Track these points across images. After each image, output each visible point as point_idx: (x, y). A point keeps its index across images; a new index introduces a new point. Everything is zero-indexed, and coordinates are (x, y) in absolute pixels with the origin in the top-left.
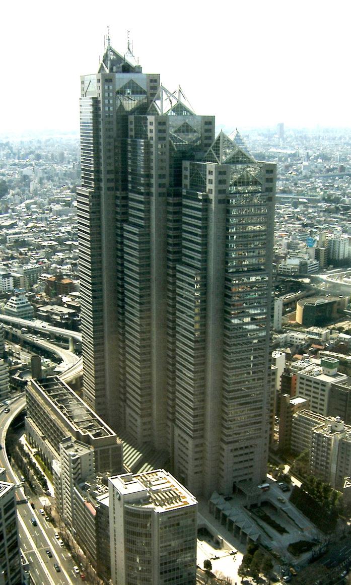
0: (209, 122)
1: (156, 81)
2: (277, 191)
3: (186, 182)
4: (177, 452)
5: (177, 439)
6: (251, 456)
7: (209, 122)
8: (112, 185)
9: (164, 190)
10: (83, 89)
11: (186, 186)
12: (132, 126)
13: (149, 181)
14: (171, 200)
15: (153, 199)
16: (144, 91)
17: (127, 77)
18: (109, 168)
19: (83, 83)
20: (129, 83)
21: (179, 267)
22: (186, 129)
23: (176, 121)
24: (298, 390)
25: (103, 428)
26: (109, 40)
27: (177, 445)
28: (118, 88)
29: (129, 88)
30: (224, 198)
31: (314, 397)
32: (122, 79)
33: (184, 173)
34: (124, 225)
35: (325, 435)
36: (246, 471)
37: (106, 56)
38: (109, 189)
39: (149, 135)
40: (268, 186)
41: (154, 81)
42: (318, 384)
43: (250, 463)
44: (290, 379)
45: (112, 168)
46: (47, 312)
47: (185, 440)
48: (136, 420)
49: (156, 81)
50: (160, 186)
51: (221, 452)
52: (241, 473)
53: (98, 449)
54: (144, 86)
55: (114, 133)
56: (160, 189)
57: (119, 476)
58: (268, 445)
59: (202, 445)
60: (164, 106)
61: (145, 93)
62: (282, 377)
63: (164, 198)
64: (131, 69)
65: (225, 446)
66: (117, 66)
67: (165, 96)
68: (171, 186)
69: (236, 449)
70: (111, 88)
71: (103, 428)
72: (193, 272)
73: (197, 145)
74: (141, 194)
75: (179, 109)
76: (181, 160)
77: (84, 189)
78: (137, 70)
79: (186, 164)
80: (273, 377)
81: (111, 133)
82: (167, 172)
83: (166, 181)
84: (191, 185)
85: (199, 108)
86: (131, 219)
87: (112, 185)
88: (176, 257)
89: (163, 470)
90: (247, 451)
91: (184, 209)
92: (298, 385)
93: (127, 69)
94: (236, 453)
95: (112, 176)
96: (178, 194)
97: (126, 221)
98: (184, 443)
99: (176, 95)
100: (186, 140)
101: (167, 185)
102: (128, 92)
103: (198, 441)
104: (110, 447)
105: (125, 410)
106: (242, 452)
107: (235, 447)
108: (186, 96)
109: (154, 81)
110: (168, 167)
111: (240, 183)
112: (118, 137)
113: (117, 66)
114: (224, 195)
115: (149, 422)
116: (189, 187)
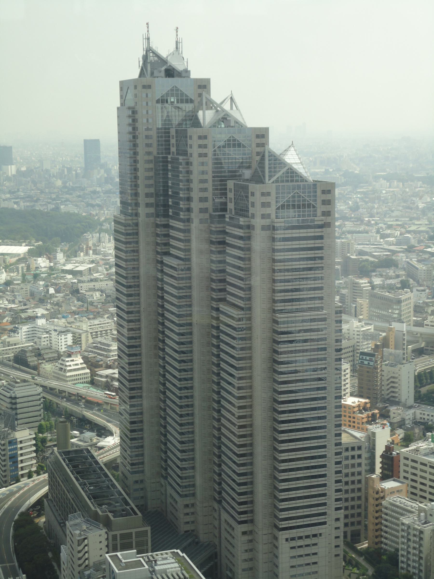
0: (262, 135)
2: (337, 216)
5: (224, 526)
6: (313, 550)
7: (262, 135)
10: (121, 97)
11: (231, 210)
12: (173, 141)
13: (189, 204)
16: (191, 99)
17: (171, 82)
18: (148, 190)
19: (121, 89)
20: (172, 90)
21: (223, 307)
22: (233, 143)
23: (221, 135)
25: (128, 507)
26: (148, 39)
27: (224, 534)
28: (158, 97)
29: (172, 95)
30: (268, 224)
31: (412, 480)
32: (163, 85)
34: (164, 258)
35: (416, 526)
37: (145, 58)
40: (325, 210)
41: (204, 85)
42: (426, 465)
43: (313, 559)
44: (392, 459)
45: (152, 190)
46: (107, 376)
47: (231, 526)
48: (176, 502)
51: (275, 541)
53: (118, 533)
54: (190, 92)
55: (154, 150)
56: (202, 214)
57: (119, 554)
59: (251, 532)
60: (206, 116)
61: (192, 101)
62: (382, 456)
63: (206, 225)
65: (276, 531)
66: (158, 69)
69: (293, 539)
70: (149, 96)
71: (128, 507)
72: (235, 312)
73: (248, 161)
76: (226, 181)
78: (184, 75)
79: (230, 184)
81: (151, 149)
83: (209, 205)
84: (235, 209)
85: (251, 119)
87: (152, 210)
88: (221, 295)
89: (179, 551)
90: (308, 541)
92: (402, 468)
93: (170, 73)
94: (293, 544)
95: (152, 200)
97: (167, 254)
100: (236, 155)
101: (211, 210)
102: (172, 100)
104: (133, 531)
105: (220, 515)
106: (300, 543)
107: (292, 536)
109: (204, 85)
111: (288, 206)
112: (158, 153)
113: (158, 69)
114: (268, 220)
115: (193, 505)
116: (233, 213)
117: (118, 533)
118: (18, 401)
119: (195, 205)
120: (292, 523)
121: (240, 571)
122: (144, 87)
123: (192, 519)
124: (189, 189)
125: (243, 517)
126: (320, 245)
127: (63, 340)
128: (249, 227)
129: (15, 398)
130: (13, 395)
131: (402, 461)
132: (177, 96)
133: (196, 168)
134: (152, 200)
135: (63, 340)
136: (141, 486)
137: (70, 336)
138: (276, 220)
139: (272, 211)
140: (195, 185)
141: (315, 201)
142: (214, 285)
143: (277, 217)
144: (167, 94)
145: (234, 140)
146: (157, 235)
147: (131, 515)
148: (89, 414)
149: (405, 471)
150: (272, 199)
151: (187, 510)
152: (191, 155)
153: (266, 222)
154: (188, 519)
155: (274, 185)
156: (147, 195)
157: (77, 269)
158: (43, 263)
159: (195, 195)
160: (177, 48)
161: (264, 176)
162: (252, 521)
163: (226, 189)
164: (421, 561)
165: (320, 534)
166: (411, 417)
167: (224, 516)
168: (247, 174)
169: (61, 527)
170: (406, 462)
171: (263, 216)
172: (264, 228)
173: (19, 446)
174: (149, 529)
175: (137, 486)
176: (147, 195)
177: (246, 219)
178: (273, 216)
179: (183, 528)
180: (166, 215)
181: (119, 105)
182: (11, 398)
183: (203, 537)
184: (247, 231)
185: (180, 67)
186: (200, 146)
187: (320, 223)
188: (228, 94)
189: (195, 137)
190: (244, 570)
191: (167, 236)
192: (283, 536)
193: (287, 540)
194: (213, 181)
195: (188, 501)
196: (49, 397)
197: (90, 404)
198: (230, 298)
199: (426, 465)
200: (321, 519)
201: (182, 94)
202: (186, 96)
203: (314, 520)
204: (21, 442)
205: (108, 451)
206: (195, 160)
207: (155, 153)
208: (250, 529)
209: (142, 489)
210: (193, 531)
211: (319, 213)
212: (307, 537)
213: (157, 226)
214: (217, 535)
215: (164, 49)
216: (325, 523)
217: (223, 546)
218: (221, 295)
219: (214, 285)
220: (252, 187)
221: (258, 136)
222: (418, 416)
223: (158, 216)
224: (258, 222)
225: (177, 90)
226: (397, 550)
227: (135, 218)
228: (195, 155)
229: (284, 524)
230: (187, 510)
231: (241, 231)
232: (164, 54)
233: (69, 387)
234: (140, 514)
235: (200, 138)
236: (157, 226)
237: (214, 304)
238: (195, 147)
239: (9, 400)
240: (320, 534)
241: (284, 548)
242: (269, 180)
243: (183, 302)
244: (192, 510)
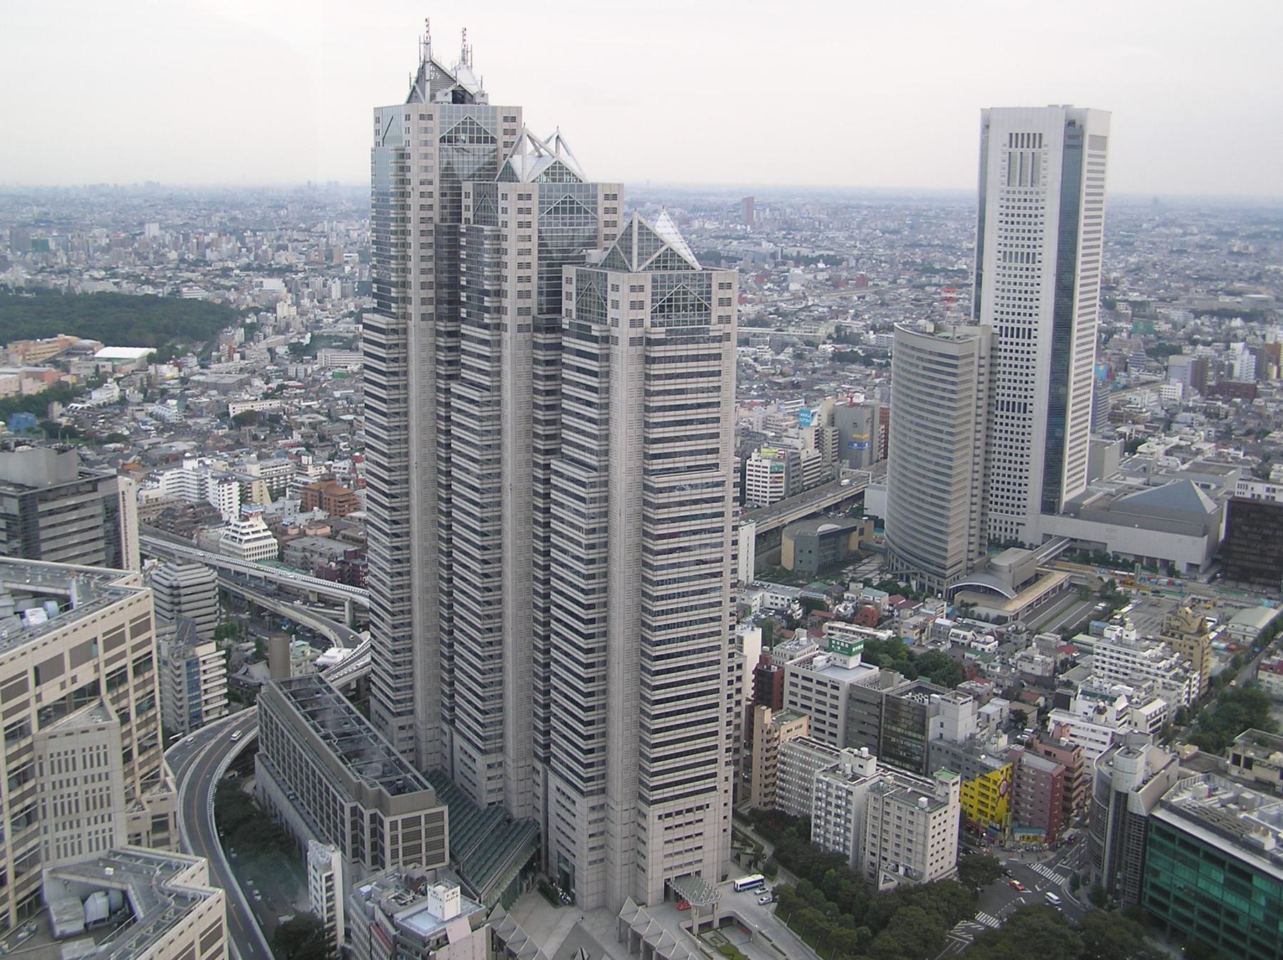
1: (514, 119)
3: (569, 305)
4: (554, 822)
5: (553, 796)
8: (431, 309)
9: (528, 320)
10: (377, 132)
11: (569, 312)
14: (541, 338)
15: (507, 336)
18: (424, 278)
19: (377, 120)
21: (556, 464)
24: (787, 698)
25: (409, 776)
27: (553, 808)
29: (465, 131)
31: (818, 711)
33: (566, 288)
36: (689, 857)
37: (422, 70)
38: (424, 317)
39: (501, 217)
41: (512, 117)
42: (826, 685)
43: (697, 842)
45: (431, 278)
49: (514, 119)
50: (521, 312)
51: (640, 820)
52: (678, 860)
53: (399, 818)
55: (435, 214)
58: (730, 805)
60: (526, 165)
62: (756, 671)
64: (467, 96)
65: (644, 808)
66: (442, 89)
67: (529, 147)
68: (541, 312)
71: (409, 776)
72: (583, 473)
74: (486, 327)
75: (557, 171)
76: (561, 265)
77: (377, 317)
79: (569, 271)
80: (737, 673)
82: (533, 286)
84: (578, 310)
86: (465, 374)
87: (431, 309)
90: (690, 817)
91: (564, 355)
92: (787, 688)
93: (460, 96)
94: (669, 822)
95: (431, 293)
96: (554, 328)
98: (568, 805)
99: (552, 145)
101: (535, 311)
103: (593, 800)
104: (422, 813)
106: (679, 820)
108: (570, 146)
109: (512, 117)
110: (535, 279)
112: (442, 220)
113: (442, 89)
114: (640, 330)
115: (500, 764)
117: (399, 818)
118: (182, 591)
119: (510, 303)
120: (668, 792)
121: (585, 865)
122: (422, 117)
123: (500, 786)
124: (500, 278)
125: (592, 786)
126: (717, 369)
127: (226, 492)
128: (499, 327)
129: (178, 588)
130: (175, 584)
131: (788, 679)
132: (472, 131)
133: (512, 245)
134: (431, 293)
135: (226, 492)
136: (410, 734)
137: (235, 485)
138: (653, 330)
139: (646, 315)
140: (511, 272)
141: (709, 299)
142: (540, 429)
143: (653, 325)
144: (457, 130)
145: (572, 202)
146: (536, 361)
147: (413, 789)
148: (284, 609)
149: (792, 693)
150: (646, 296)
151: (492, 773)
152: (505, 224)
153: (637, 332)
154: (493, 785)
155: (649, 275)
156: (424, 286)
157: (223, 381)
158: (168, 371)
159: (511, 287)
160: (464, 60)
161: (630, 261)
162: (603, 791)
163: (560, 278)
164: (848, 834)
165: (708, 806)
166: (758, 602)
167: (554, 781)
168: (596, 255)
169: (291, 801)
170: (794, 680)
171: (633, 323)
172: (633, 342)
173: (202, 668)
174: (445, 809)
175: (403, 734)
176: (424, 286)
177: (604, 327)
178: (648, 323)
179: (485, 799)
180: (454, 317)
181: (372, 145)
182: (171, 587)
183: (517, 813)
184: (495, 332)
185: (472, 89)
186: (520, 211)
187: (717, 334)
188: (551, 131)
189: (513, 197)
190: (590, 863)
191: (456, 349)
192: (654, 812)
193: (660, 817)
194: (540, 265)
195: (492, 759)
196: (228, 585)
197: (283, 592)
198: (566, 449)
199: (826, 685)
200: (709, 783)
201: (479, 130)
202: (486, 132)
203: (700, 785)
204: (204, 662)
205: (334, 672)
206: (512, 232)
207: (437, 219)
208: (601, 802)
209: (411, 738)
210: (500, 802)
211: (714, 319)
212: (689, 811)
213: (438, 333)
214: (541, 809)
215: (447, 58)
216: (714, 788)
217: (552, 824)
218: (550, 445)
219: (540, 429)
220: (613, 277)
221: (607, 197)
222: (768, 601)
223: (440, 318)
224: (624, 332)
225: (472, 123)
226: (809, 817)
227: (402, 321)
228: (513, 225)
229: (658, 795)
230: (492, 773)
231: (595, 345)
232: (447, 66)
233: (248, 567)
234: (431, 788)
235: (520, 197)
236: (438, 333)
237: (540, 459)
238: (512, 212)
239: (168, 591)
240: (708, 806)
241: (656, 832)
242: (639, 266)
243: (395, 436)
244: (499, 772)
